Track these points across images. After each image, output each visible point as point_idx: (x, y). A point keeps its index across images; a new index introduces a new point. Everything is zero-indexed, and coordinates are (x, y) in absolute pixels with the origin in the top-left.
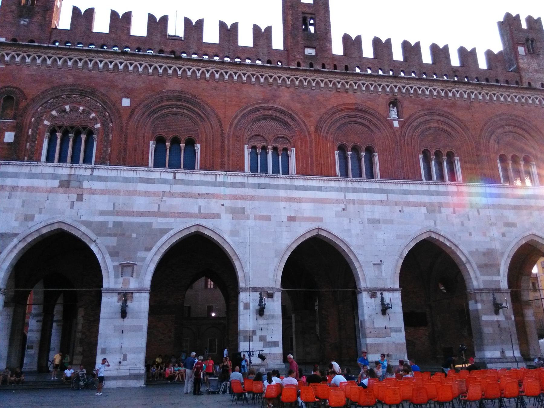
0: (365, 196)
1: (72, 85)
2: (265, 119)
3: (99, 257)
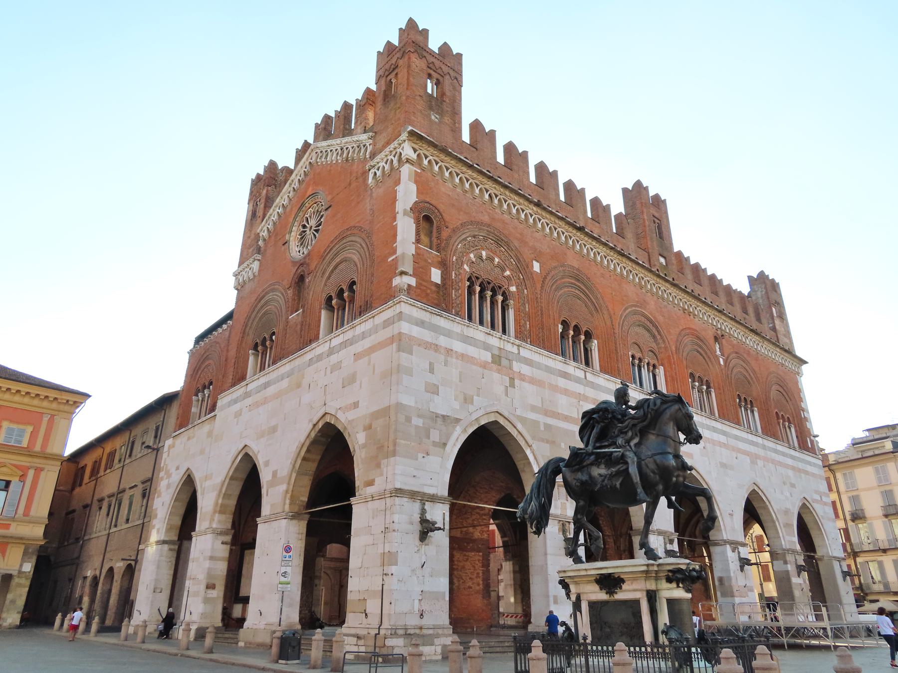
1: (489, 226)
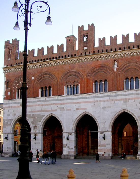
0: (101, 99)
2: (71, 76)
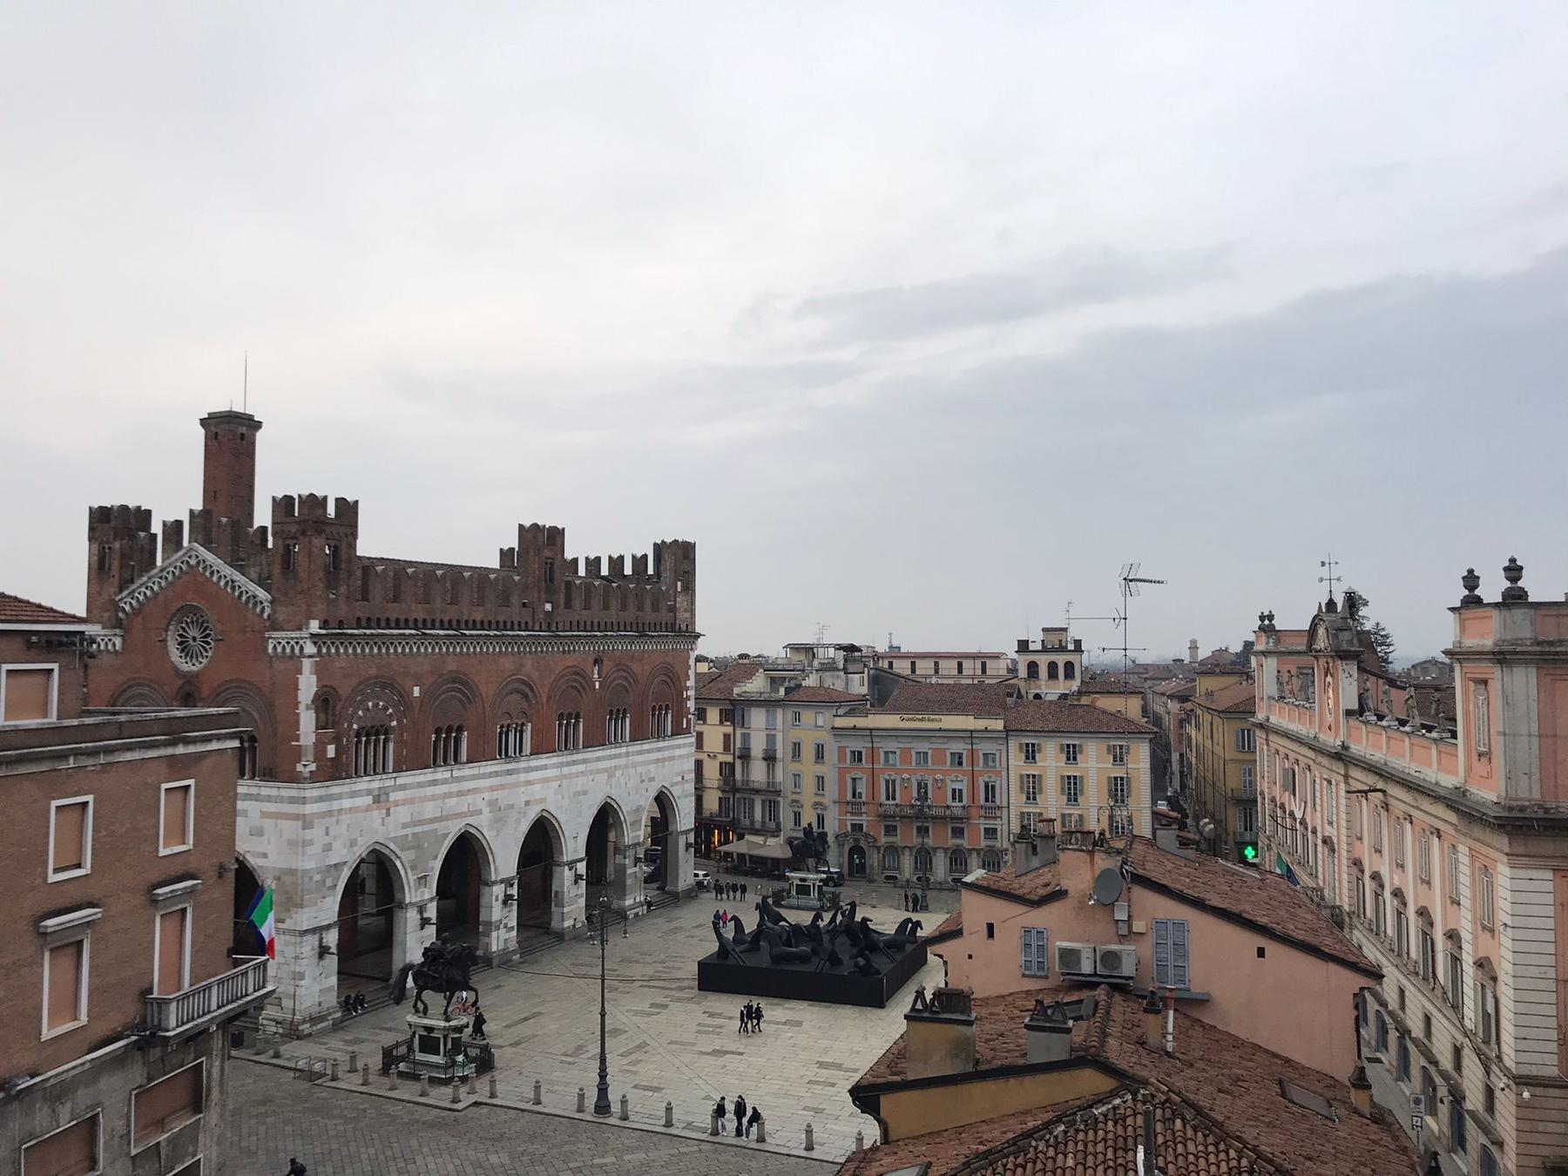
0: (574, 769)
3: (402, 872)
